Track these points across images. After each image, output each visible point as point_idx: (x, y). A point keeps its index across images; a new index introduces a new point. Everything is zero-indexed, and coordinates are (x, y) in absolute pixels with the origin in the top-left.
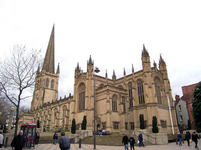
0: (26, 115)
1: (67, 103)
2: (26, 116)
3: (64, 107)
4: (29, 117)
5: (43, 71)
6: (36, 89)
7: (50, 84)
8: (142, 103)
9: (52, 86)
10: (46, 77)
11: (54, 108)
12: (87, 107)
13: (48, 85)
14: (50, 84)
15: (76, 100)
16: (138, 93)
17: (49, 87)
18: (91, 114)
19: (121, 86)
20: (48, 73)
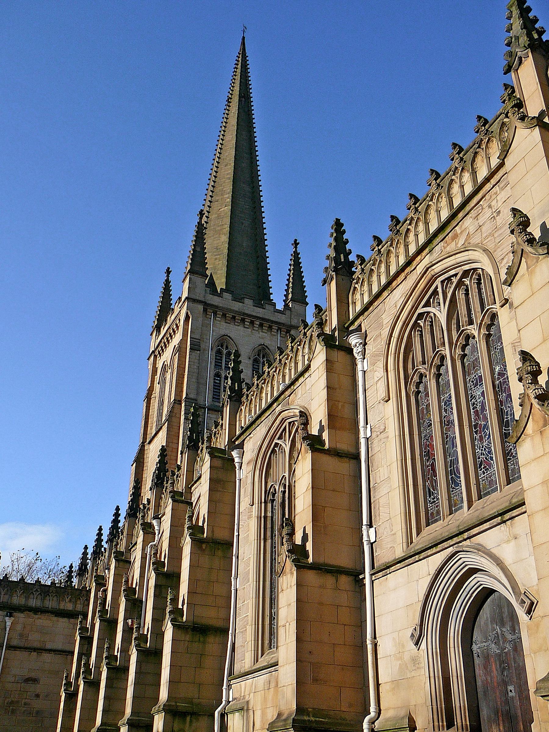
4: (43, 621)
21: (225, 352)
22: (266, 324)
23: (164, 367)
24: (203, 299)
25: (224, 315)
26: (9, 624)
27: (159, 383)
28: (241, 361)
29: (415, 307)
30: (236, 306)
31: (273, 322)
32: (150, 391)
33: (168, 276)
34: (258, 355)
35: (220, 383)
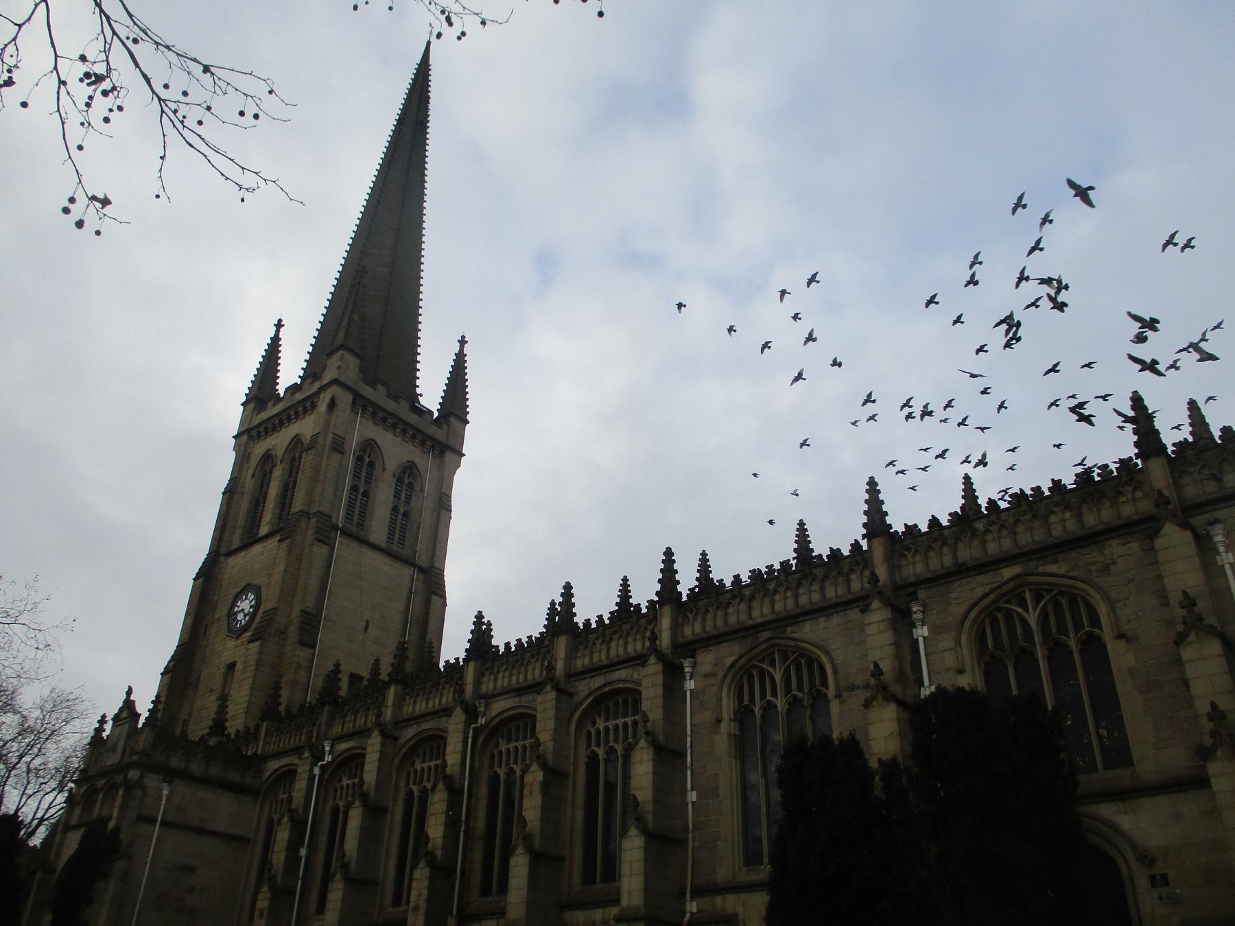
0: (176, 762)
2: (170, 775)
5: (334, 360)
7: (384, 494)
9: (402, 518)
10: (361, 430)
13: (364, 507)
14: (384, 494)
17: (378, 529)
20: (378, 395)
21: (367, 460)
23: (267, 457)
24: (354, 387)
25: (374, 414)
26: (165, 792)
27: (253, 476)
28: (698, 566)
29: (996, 601)
30: (390, 405)
31: (427, 435)
33: (278, 331)
34: (404, 473)
35: (355, 500)
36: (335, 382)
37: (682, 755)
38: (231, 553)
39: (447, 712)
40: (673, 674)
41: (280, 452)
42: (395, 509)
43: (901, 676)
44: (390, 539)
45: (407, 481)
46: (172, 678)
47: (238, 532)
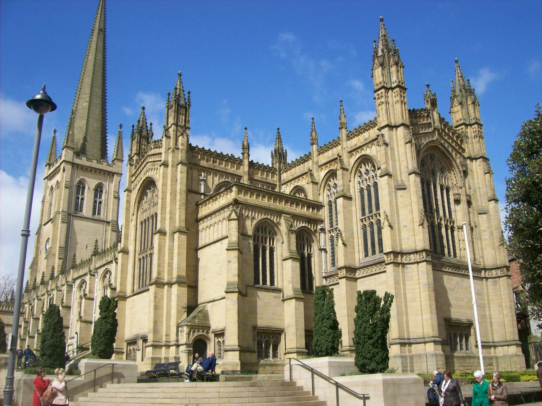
1: (111, 262)
3: (105, 277)
6: (45, 220)
8: (374, 253)
11: (78, 282)
12: (159, 273)
15: (131, 248)
16: (359, 212)
18: (174, 298)
19: (299, 189)
20: (83, 161)
21: (81, 186)
22: (102, 172)
23: (52, 188)
25: (82, 168)
30: (87, 164)
31: (105, 171)
32: (44, 197)
36: (64, 161)
37: (71, 307)
38: (45, 225)
39: (44, 295)
40: (70, 286)
41: (54, 187)
42: (95, 202)
43: (91, 291)
44: (94, 213)
45: (99, 190)
46: (31, 270)
47: (47, 218)
